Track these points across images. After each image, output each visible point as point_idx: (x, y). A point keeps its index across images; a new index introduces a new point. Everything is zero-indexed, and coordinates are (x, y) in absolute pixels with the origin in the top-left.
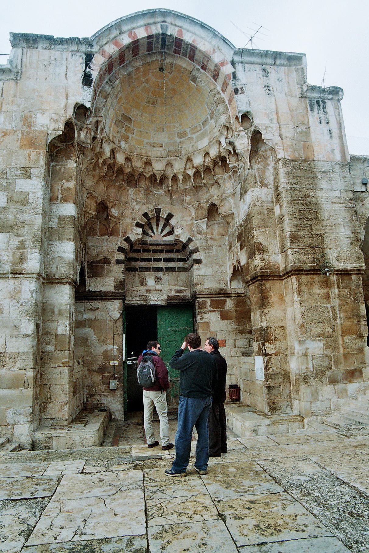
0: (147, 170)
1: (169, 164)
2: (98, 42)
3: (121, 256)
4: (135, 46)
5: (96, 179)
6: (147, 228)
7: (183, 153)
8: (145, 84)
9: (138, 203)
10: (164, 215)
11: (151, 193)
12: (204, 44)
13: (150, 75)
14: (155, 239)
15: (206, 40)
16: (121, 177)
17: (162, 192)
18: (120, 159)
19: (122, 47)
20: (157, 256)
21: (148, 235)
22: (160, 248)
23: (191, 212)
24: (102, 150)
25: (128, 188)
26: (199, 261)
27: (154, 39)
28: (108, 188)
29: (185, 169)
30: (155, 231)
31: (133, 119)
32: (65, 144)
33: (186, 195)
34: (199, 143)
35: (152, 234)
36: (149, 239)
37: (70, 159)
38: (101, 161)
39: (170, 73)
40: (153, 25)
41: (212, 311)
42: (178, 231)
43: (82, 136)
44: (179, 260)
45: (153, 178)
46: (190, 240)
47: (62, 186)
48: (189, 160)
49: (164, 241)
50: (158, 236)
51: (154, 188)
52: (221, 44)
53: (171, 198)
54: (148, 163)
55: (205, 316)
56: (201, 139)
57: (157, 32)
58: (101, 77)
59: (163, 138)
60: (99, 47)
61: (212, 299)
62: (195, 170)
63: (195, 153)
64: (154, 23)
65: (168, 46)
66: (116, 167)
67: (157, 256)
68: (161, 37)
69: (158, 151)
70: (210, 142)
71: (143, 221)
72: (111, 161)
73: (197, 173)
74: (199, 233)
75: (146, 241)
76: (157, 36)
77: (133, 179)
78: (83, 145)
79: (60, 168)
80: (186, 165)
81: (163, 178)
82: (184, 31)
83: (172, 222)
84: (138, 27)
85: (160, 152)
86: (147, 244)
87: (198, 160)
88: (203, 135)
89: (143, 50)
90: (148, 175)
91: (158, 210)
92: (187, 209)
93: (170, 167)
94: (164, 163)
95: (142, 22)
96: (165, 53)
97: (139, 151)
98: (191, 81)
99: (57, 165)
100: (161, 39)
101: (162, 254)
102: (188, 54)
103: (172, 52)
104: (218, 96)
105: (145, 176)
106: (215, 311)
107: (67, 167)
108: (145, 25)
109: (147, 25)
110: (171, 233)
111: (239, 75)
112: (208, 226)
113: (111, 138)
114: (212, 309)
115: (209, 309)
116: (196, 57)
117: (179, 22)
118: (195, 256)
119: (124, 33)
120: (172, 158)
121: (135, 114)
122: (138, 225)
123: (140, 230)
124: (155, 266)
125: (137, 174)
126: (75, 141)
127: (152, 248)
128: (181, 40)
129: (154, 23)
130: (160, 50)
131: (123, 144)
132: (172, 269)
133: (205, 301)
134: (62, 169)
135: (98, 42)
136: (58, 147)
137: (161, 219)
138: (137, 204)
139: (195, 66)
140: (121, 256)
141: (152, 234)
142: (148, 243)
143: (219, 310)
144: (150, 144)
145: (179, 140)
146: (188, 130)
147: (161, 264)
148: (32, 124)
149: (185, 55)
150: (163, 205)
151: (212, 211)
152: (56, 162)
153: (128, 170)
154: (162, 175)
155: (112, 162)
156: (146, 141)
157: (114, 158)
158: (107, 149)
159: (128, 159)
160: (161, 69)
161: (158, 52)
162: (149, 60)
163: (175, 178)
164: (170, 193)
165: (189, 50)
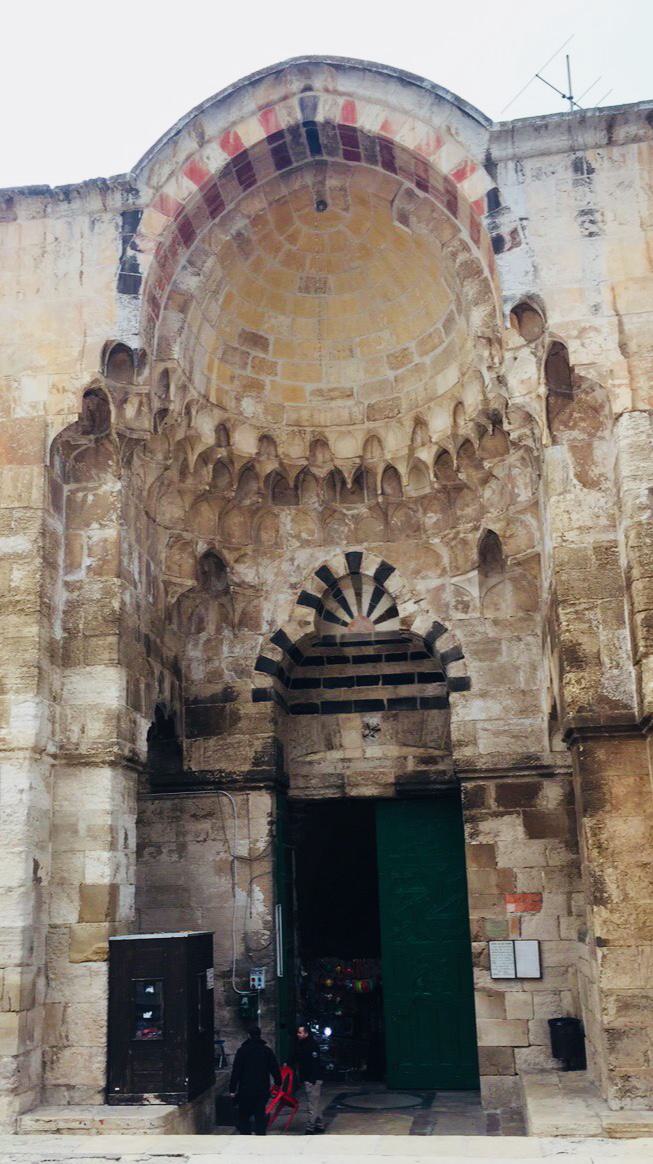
0: (320, 457)
1: (372, 439)
2: (149, 178)
3: (265, 681)
4: (242, 168)
5: (189, 499)
6: (332, 605)
7: (404, 406)
8: (287, 246)
9: (305, 544)
10: (369, 568)
11: (337, 515)
12: (412, 130)
13: (298, 223)
14: (355, 629)
15: (415, 117)
16: (254, 486)
17: (362, 509)
18: (245, 443)
19: (206, 179)
20: (366, 670)
21: (332, 618)
22: (370, 651)
23: (438, 556)
24: (192, 432)
25: (276, 510)
26: (462, 684)
27: (288, 138)
28: (223, 515)
29: (412, 449)
30: (354, 609)
31: (272, 339)
32: (92, 437)
33: (425, 512)
34: (439, 378)
35: (347, 619)
36: (338, 631)
37: (106, 471)
38: (193, 458)
39: (346, 209)
40: (282, 104)
41: (502, 815)
42: (406, 609)
43: (130, 415)
44: (426, 678)
45: (336, 475)
46: (438, 629)
47: (89, 538)
48: (420, 423)
49: (378, 634)
50: (360, 622)
51: (343, 501)
52: (457, 120)
53: (387, 523)
54: (319, 443)
55: (484, 826)
56: (442, 370)
57: (292, 122)
58: (165, 259)
59: (351, 374)
60: (151, 191)
62: (435, 449)
63: (432, 404)
64: (285, 98)
65: (326, 146)
66: (238, 466)
67: (366, 670)
68: (303, 130)
69: (343, 408)
70: (463, 375)
71: (314, 587)
72: (222, 453)
73: (442, 456)
74: (466, 607)
75: (334, 637)
76: (294, 130)
77: (285, 487)
78: (135, 436)
79: (86, 496)
80: (412, 440)
81: (361, 475)
82: (359, 105)
83: (393, 584)
84: (242, 119)
85: (347, 411)
86: (335, 644)
87: (440, 424)
88: (448, 355)
89: (266, 172)
90: (321, 472)
91: (354, 560)
92: (428, 548)
93: (375, 443)
94: (360, 438)
95: (251, 102)
96: (325, 163)
97: (294, 416)
98: (397, 224)
99: (78, 490)
100: (304, 135)
101: (378, 665)
102: (379, 158)
103: (340, 159)
104: (462, 257)
105: (314, 476)
106: (510, 813)
107: (100, 492)
108: (260, 108)
109: (266, 110)
110: (392, 612)
111: (507, 197)
112: (487, 590)
113: (213, 399)
114: (501, 809)
116: (398, 163)
117: (345, 84)
118: (454, 670)
119: (209, 141)
120: (377, 424)
121: (275, 325)
122: (305, 599)
123: (309, 613)
124: (362, 697)
125: (293, 474)
126: (114, 432)
127: (351, 652)
128: (354, 130)
129: (285, 98)
130: (310, 159)
131: (249, 406)
132: (408, 703)
133: (482, 789)
134: (90, 498)
135: (149, 178)
136: (79, 446)
137: (364, 580)
138: (301, 546)
139: (401, 184)
140: (265, 681)
141: (347, 619)
142: (338, 640)
144: (319, 392)
145: (391, 374)
146: (413, 346)
147: (382, 693)
148: (13, 406)
149: (372, 159)
150: (365, 544)
151: (490, 552)
152: (77, 480)
153: (269, 466)
154: (359, 468)
155: (225, 454)
156: (309, 387)
157: (229, 444)
158: (206, 426)
159: (266, 439)
160: (322, 205)
161: (308, 165)
162: (284, 190)
163: (391, 471)
164: (383, 512)
165: (378, 148)
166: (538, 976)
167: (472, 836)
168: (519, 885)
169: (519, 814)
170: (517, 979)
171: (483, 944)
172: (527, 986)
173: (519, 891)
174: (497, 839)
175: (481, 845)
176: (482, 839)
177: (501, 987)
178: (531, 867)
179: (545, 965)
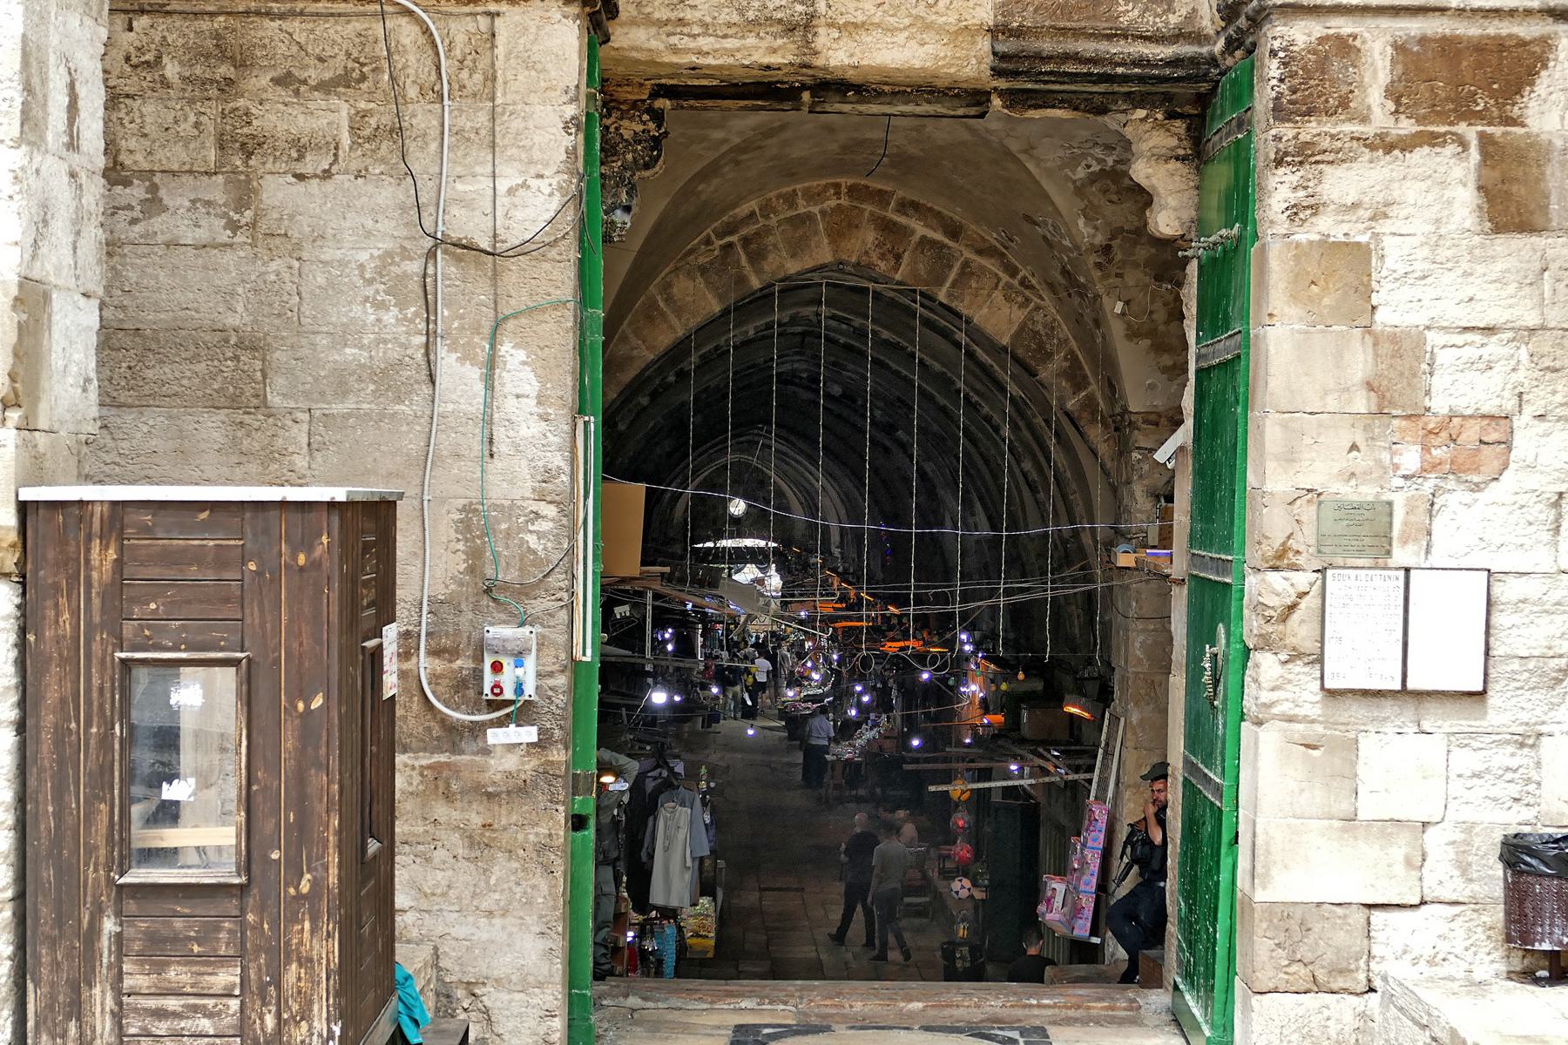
41: (1406, 145)
55: (1342, 183)
61: (1414, 27)
106: (1433, 140)
114: (1407, 127)
115: (1381, 117)
133: (1345, 47)
143: (1470, 132)
166: (1480, 689)
167: (1294, 211)
168: (1438, 382)
169: (1464, 145)
170: (1404, 693)
171: (1302, 580)
172: (1441, 722)
173: (1440, 404)
174: (1384, 227)
175: (1328, 247)
176: (1328, 225)
177: (1357, 711)
178: (1489, 330)
179: (1498, 650)
